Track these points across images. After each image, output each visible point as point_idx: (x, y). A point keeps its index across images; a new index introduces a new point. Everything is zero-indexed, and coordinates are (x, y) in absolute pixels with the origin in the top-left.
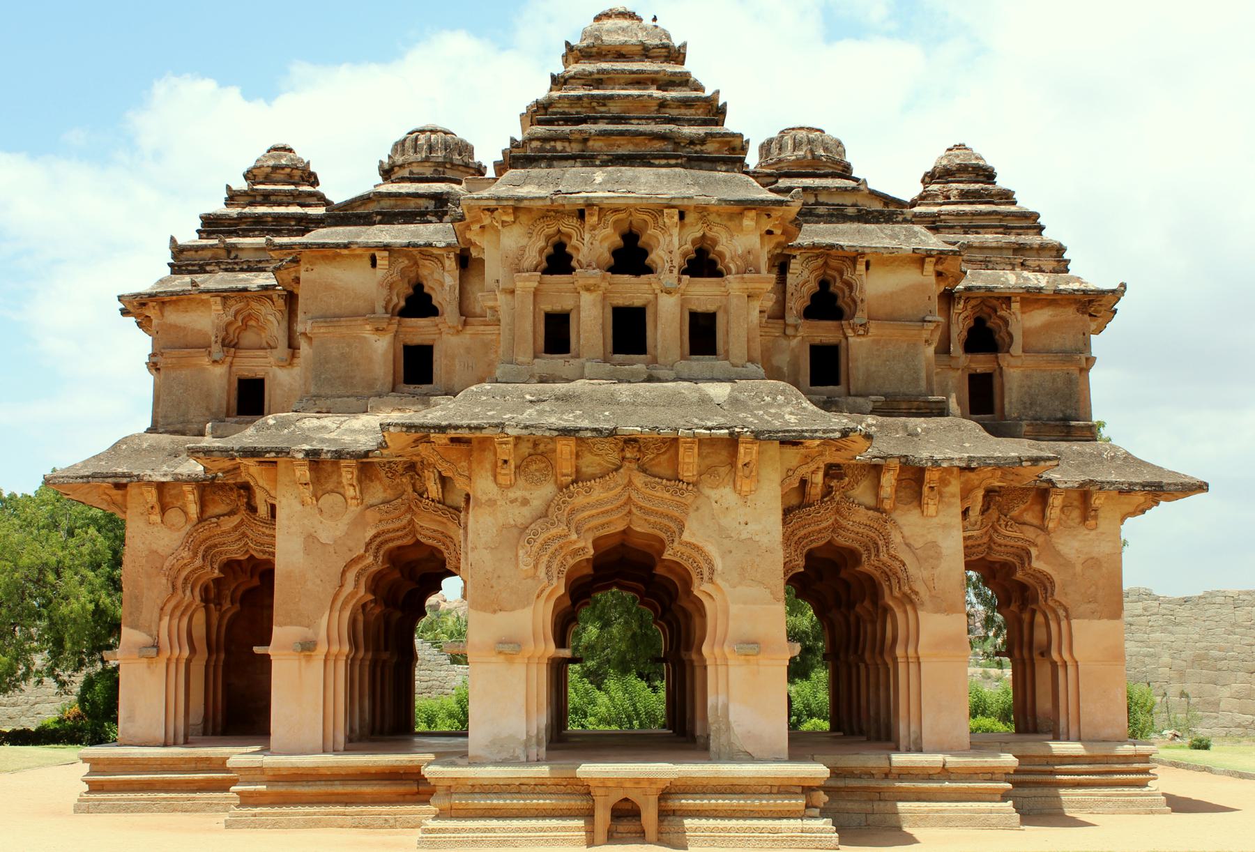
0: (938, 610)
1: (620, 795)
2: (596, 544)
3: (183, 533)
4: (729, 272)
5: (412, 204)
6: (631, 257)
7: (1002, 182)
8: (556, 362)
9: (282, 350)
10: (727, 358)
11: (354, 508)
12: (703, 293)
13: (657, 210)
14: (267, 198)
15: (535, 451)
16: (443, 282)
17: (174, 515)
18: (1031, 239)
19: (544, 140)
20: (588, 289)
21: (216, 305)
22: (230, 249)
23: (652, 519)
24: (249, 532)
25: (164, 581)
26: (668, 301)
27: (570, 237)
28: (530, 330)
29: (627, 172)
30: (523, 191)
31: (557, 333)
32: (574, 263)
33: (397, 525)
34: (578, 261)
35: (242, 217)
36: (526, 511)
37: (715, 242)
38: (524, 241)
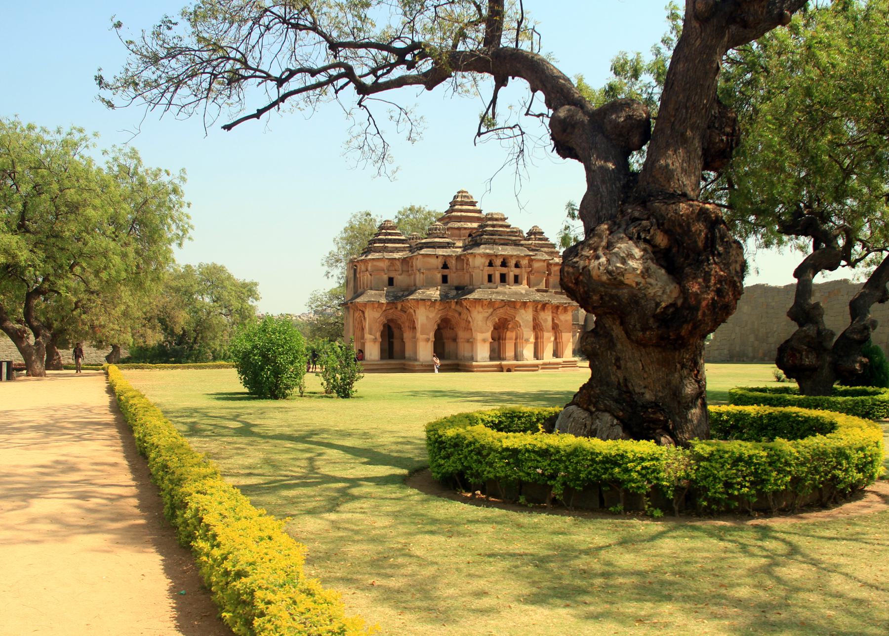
6: (504, 264)
7: (546, 235)
8: (490, 285)
9: (400, 272)
12: (517, 271)
13: (512, 256)
14: (390, 234)
15: (491, 303)
16: (452, 263)
17: (379, 309)
18: (553, 250)
26: (512, 272)
28: (486, 278)
29: (506, 247)
30: (488, 251)
31: (490, 278)
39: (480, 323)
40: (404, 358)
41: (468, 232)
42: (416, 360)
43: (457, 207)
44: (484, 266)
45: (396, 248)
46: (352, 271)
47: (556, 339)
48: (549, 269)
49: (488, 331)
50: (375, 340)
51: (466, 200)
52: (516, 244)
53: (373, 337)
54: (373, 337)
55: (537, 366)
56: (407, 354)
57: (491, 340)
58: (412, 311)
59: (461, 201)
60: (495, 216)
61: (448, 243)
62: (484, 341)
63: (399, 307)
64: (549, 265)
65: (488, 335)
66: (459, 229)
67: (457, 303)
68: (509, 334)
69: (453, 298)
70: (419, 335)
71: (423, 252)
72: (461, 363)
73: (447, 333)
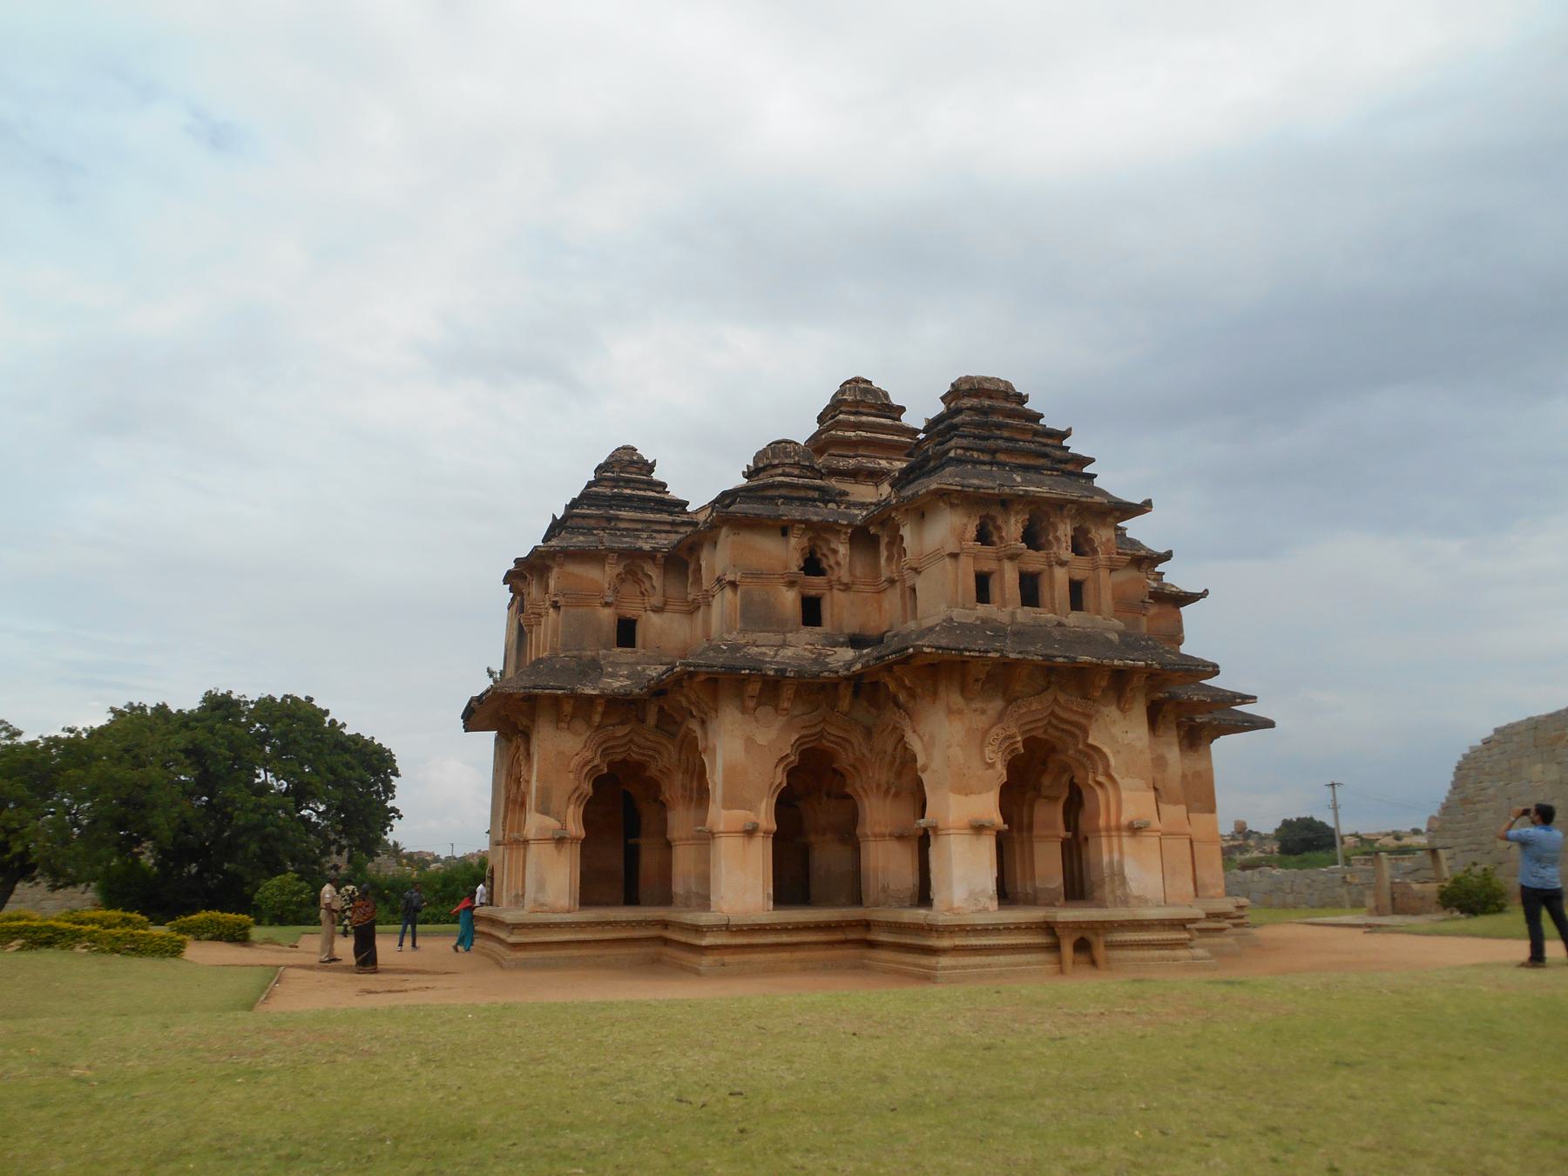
0: (1168, 803)
1: (1078, 935)
2: (1027, 742)
3: (584, 737)
4: (1095, 551)
5: (802, 494)
6: (1032, 538)
10: (1098, 612)
11: (781, 720)
12: (1080, 568)
17: (579, 725)
19: (966, 449)
20: (1012, 558)
21: (612, 558)
22: (609, 519)
23: (1065, 726)
24: (636, 739)
25: (571, 776)
27: (993, 519)
29: (1035, 477)
32: (995, 538)
33: (813, 731)
34: (1001, 538)
35: (614, 496)
36: (983, 718)
37: (1087, 531)
38: (965, 520)
40: (667, 899)
44: (961, 539)
51: (870, 399)
54: (551, 822)
55: (1180, 924)
56: (678, 888)
57: (997, 819)
58: (694, 725)
60: (987, 386)
62: (978, 829)
63: (652, 719)
65: (987, 806)
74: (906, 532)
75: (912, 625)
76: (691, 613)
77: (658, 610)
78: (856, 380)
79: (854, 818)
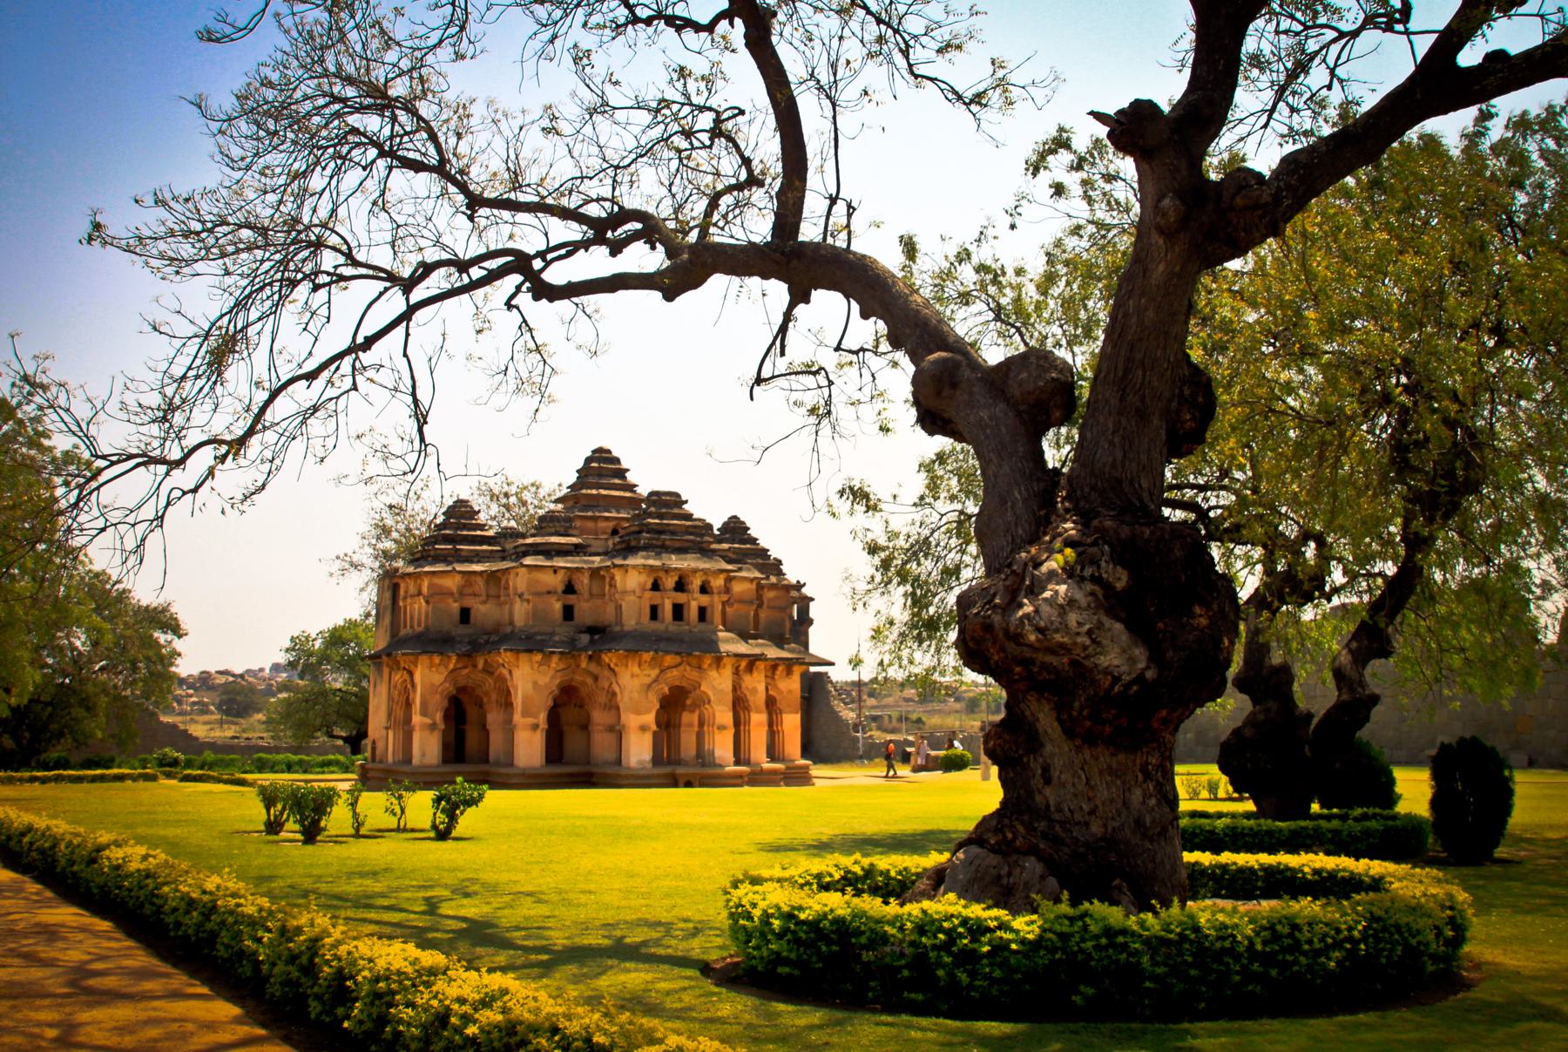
6: (680, 586)
9: (484, 597)
11: (552, 672)
12: (704, 600)
13: (695, 571)
14: (465, 527)
16: (584, 582)
17: (442, 669)
21: (458, 578)
28: (648, 611)
30: (651, 562)
39: (635, 695)
40: (487, 761)
41: (611, 524)
42: (511, 764)
43: (591, 480)
44: (644, 590)
45: (477, 553)
46: (388, 595)
47: (770, 725)
48: (760, 597)
49: (649, 711)
50: (433, 727)
52: (706, 552)
53: (429, 721)
56: (492, 757)
57: (654, 727)
58: (505, 672)
59: (602, 468)
61: (576, 546)
62: (643, 728)
64: (760, 587)
65: (650, 718)
66: (595, 519)
67: (590, 658)
68: (687, 717)
69: (585, 649)
70: (517, 718)
71: (528, 561)
72: (595, 770)
73: (569, 715)
74: (618, 578)
75: (618, 629)
76: (501, 605)
77: (485, 603)
78: (600, 450)
79: (588, 718)
